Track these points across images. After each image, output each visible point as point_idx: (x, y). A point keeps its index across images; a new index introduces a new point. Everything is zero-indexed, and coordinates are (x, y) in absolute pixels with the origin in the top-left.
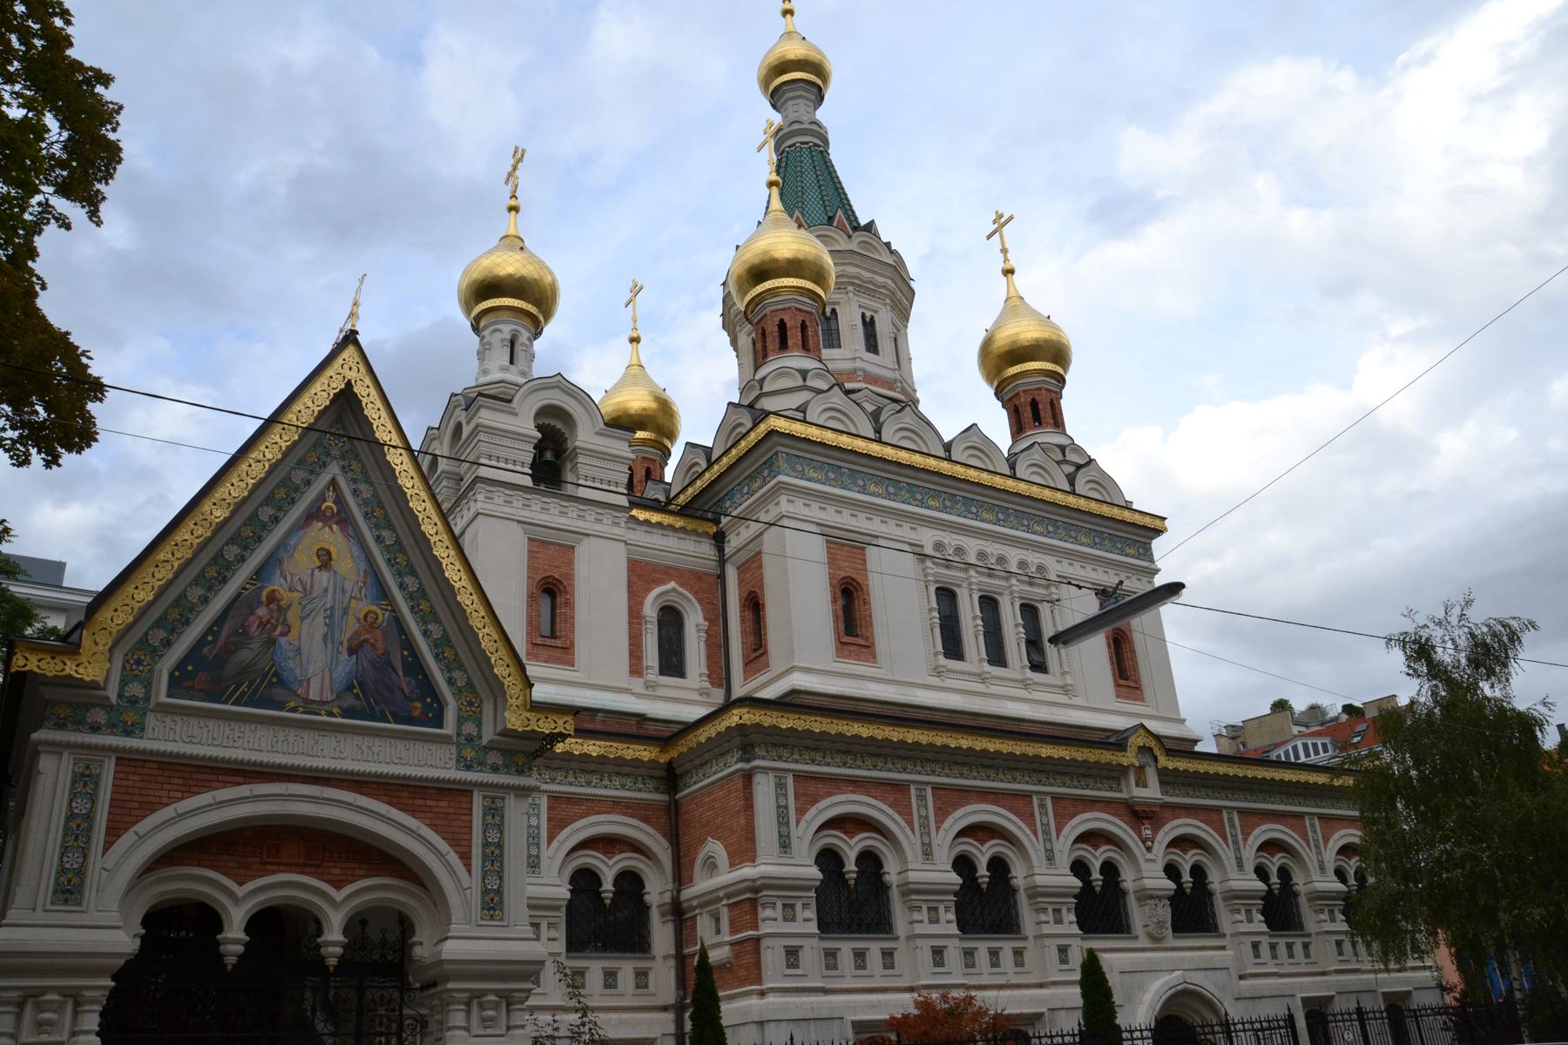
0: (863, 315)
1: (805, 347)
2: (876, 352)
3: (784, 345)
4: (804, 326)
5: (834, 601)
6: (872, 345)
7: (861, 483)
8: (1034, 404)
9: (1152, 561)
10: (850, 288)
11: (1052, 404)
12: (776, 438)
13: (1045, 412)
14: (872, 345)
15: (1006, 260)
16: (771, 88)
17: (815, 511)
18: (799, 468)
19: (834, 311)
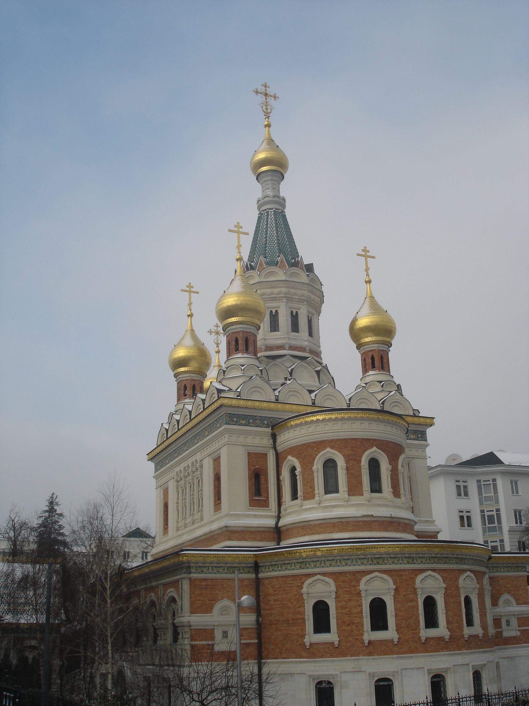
0: (292, 312)
1: (247, 350)
2: (298, 332)
3: (237, 350)
4: (247, 340)
5: (250, 479)
6: (295, 328)
7: (266, 422)
8: (373, 358)
9: (426, 440)
10: (284, 300)
11: (382, 358)
12: (223, 408)
13: (377, 363)
14: (295, 328)
15: (368, 275)
16: (257, 174)
17: (242, 439)
18: (235, 420)
19: (277, 311)
